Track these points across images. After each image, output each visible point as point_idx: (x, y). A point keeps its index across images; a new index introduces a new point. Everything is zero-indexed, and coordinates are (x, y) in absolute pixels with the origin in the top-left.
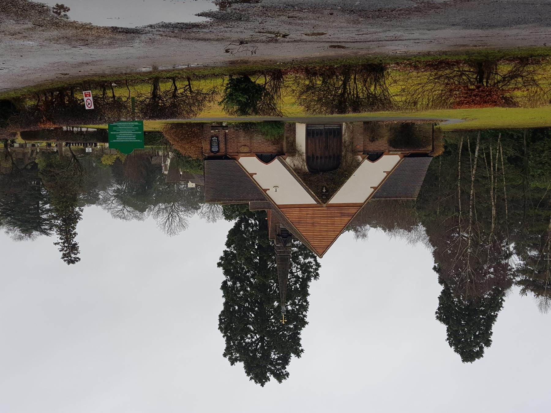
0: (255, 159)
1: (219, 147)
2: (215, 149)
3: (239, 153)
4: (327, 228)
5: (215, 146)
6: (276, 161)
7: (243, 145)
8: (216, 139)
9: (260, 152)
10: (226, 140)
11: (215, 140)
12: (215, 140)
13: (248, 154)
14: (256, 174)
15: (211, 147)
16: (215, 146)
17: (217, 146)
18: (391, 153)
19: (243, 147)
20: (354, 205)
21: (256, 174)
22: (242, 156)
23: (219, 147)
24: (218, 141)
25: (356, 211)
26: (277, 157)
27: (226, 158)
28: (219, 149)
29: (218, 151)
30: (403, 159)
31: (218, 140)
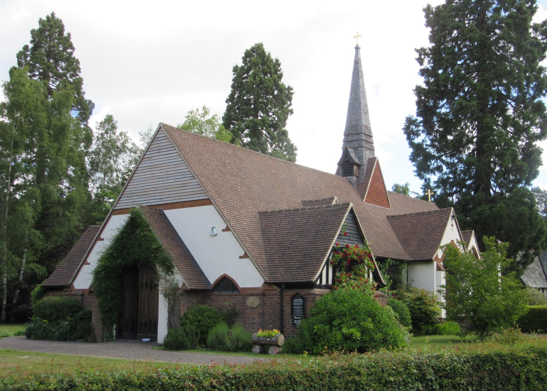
0: (242, 283)
1: (292, 306)
2: (298, 302)
3: (262, 294)
4: (153, 172)
5: (297, 308)
6: (212, 278)
7: (255, 308)
8: (295, 322)
9: (233, 297)
10: (282, 319)
11: (297, 319)
12: (297, 319)
13: (248, 292)
14: (241, 257)
15: (304, 305)
16: (297, 308)
17: (295, 307)
18: (81, 293)
19: (255, 306)
20: (120, 211)
21: (241, 257)
22: (259, 288)
23: (292, 306)
24: (293, 317)
25: (120, 202)
26: (211, 288)
27: (279, 285)
28: (292, 303)
29: (293, 297)
30: (69, 283)
31: (294, 319)
